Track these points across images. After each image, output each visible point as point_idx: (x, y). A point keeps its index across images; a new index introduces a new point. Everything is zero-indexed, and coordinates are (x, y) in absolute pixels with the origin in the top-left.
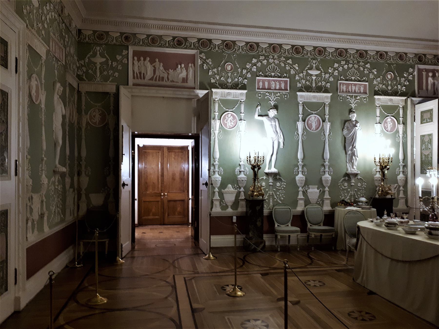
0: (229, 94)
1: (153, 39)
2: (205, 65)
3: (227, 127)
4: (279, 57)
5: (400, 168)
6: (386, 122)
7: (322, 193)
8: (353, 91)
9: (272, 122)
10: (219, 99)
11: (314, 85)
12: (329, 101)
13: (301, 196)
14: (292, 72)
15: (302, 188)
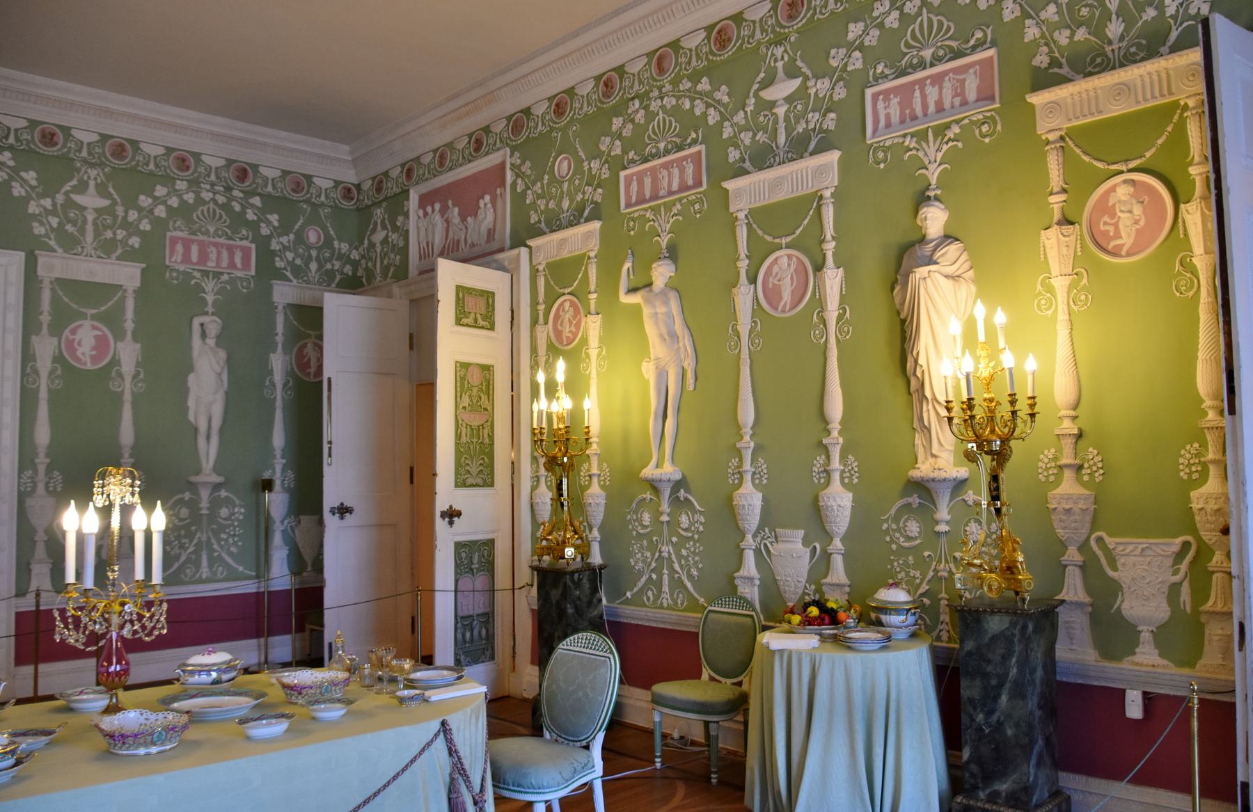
0: (563, 241)
1: (442, 157)
2: (519, 181)
3: (561, 343)
4: (675, 82)
5: (1204, 445)
6: (1103, 207)
7: (822, 563)
8: (932, 109)
9: (657, 304)
10: (548, 265)
11: (782, 139)
12: (833, 179)
13: (750, 567)
14: (713, 117)
15: (754, 536)
